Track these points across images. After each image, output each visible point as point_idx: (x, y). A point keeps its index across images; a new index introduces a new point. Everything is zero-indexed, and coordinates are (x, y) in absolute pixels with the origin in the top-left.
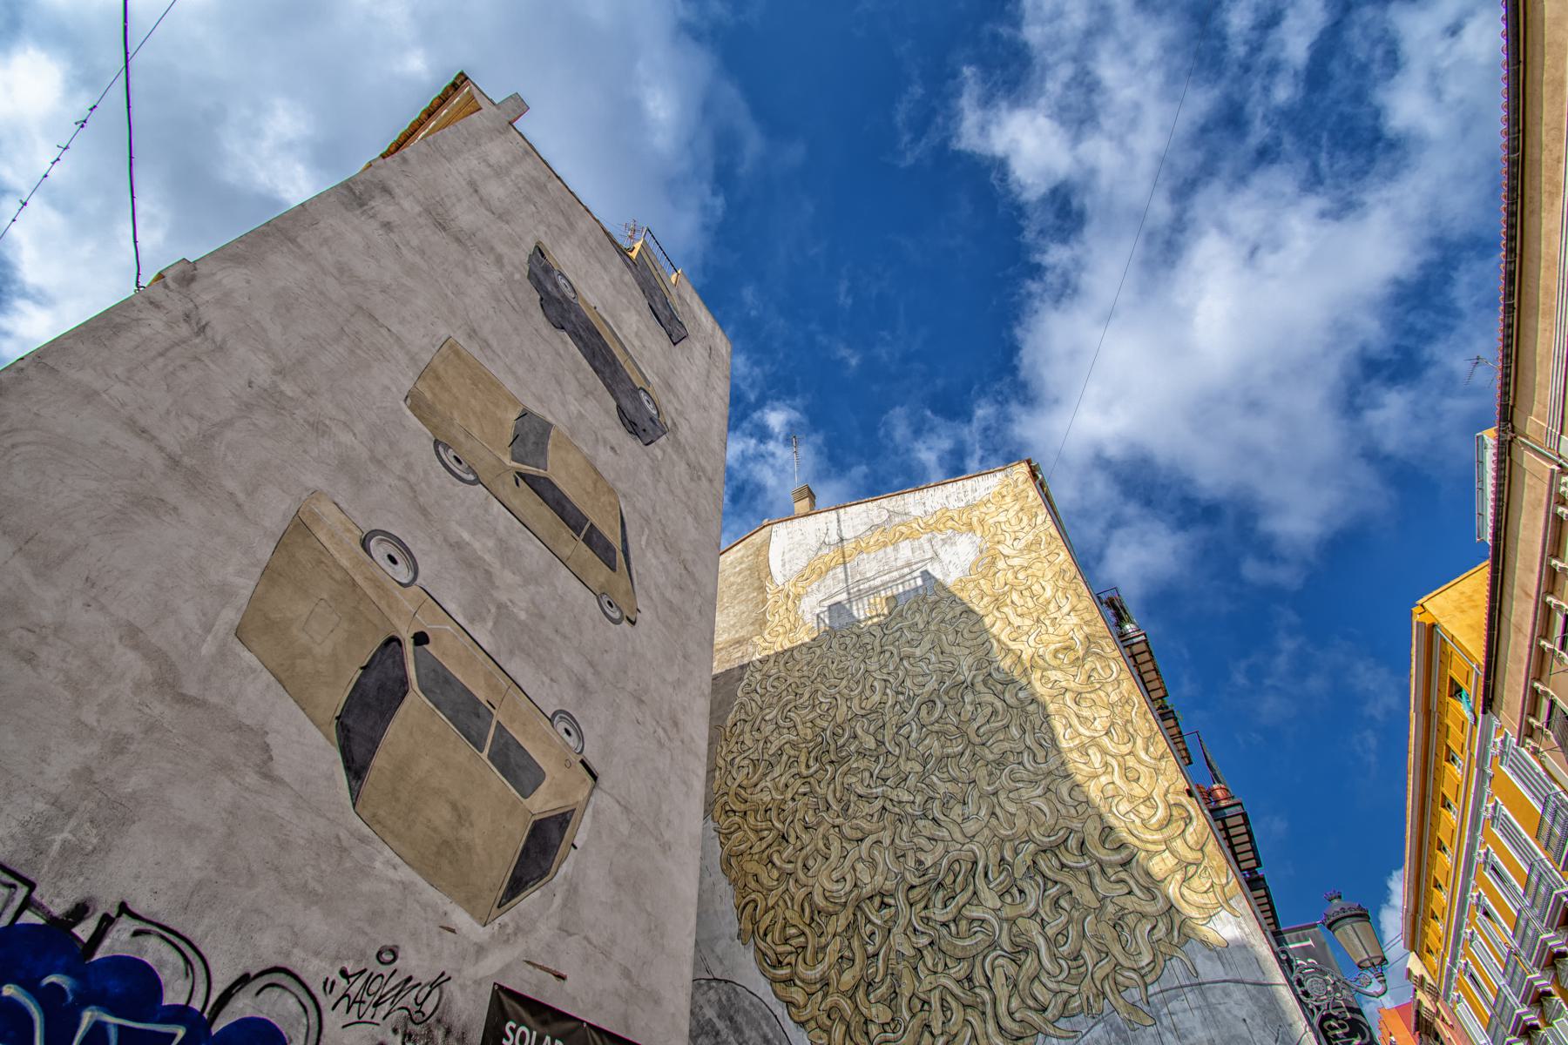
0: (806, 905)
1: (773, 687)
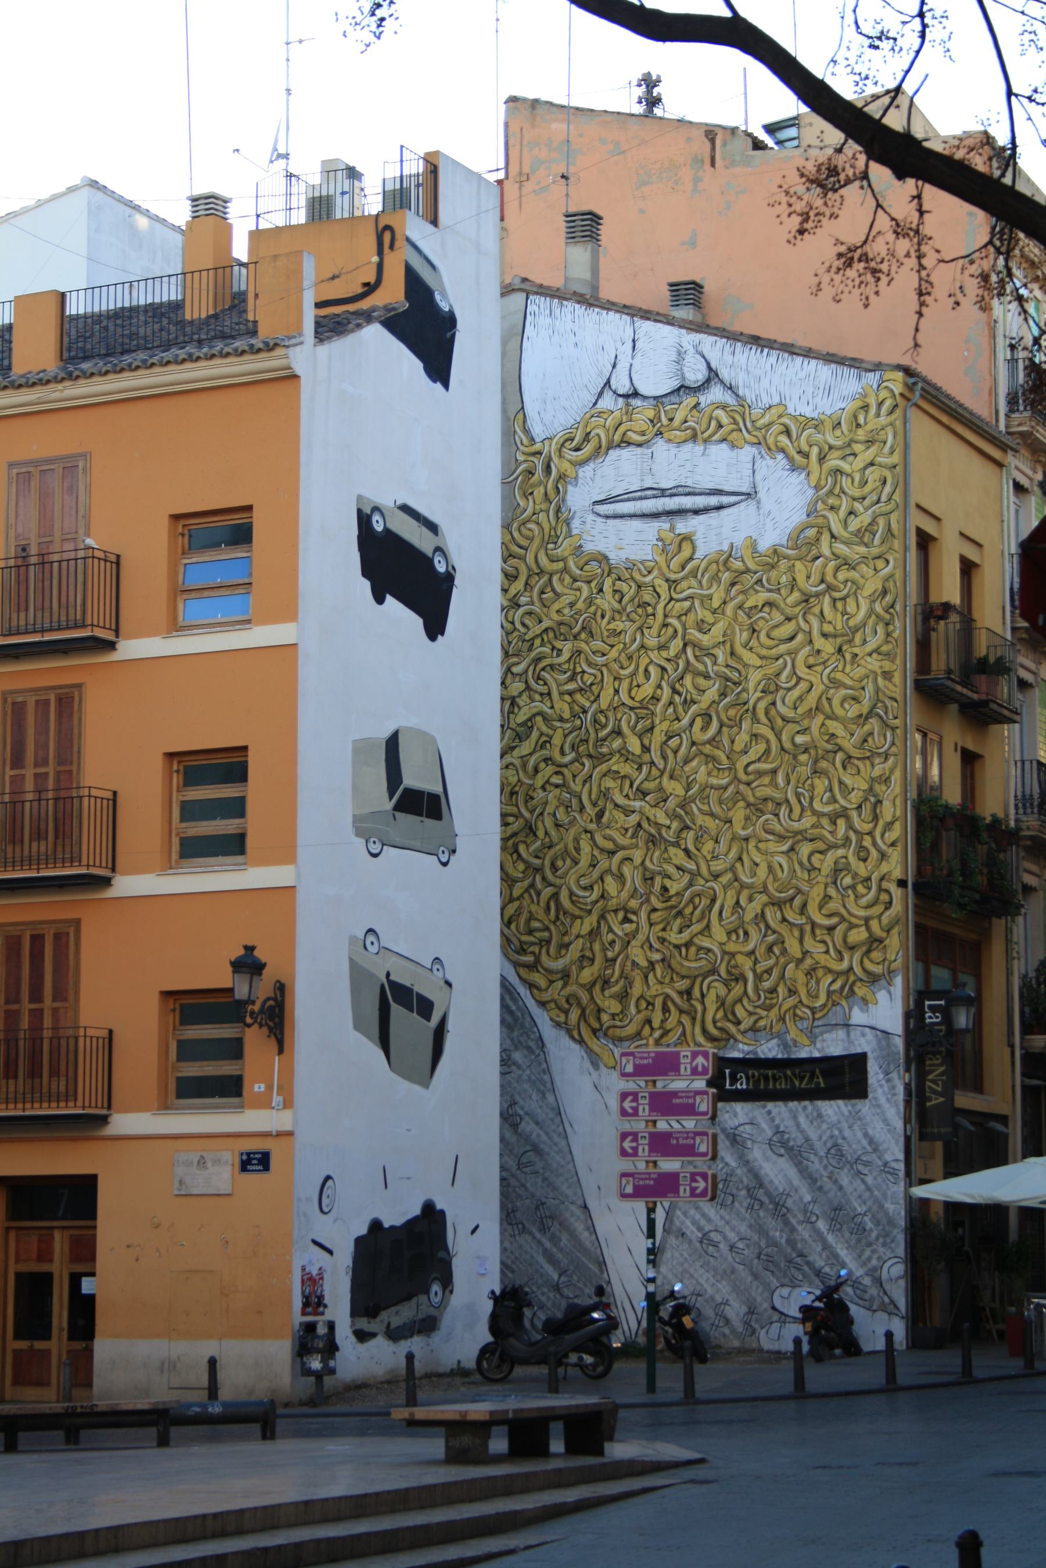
0: (552, 905)
1: (523, 624)
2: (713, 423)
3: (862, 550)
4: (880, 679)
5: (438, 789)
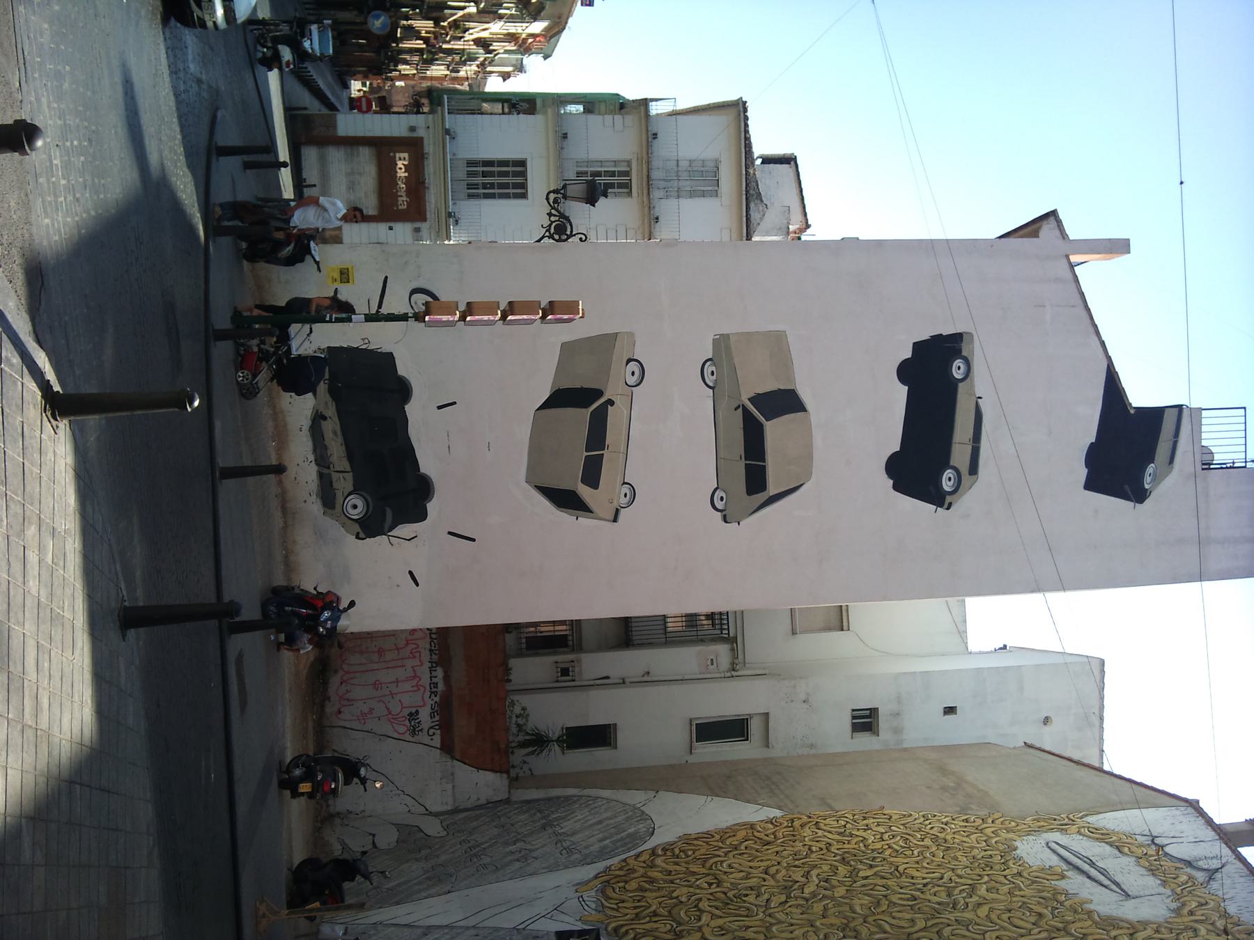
5: (772, 490)
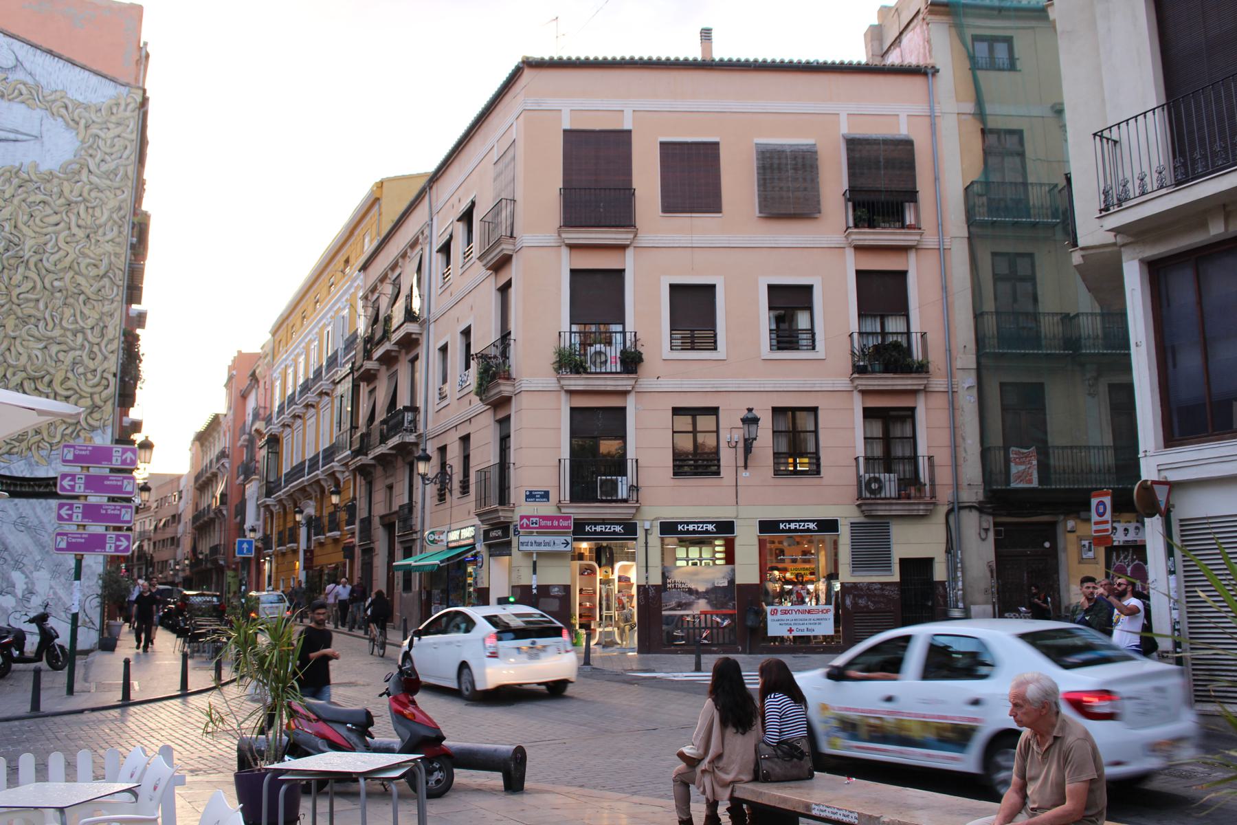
2: (16, 92)
3: (108, 182)
4: (112, 257)
